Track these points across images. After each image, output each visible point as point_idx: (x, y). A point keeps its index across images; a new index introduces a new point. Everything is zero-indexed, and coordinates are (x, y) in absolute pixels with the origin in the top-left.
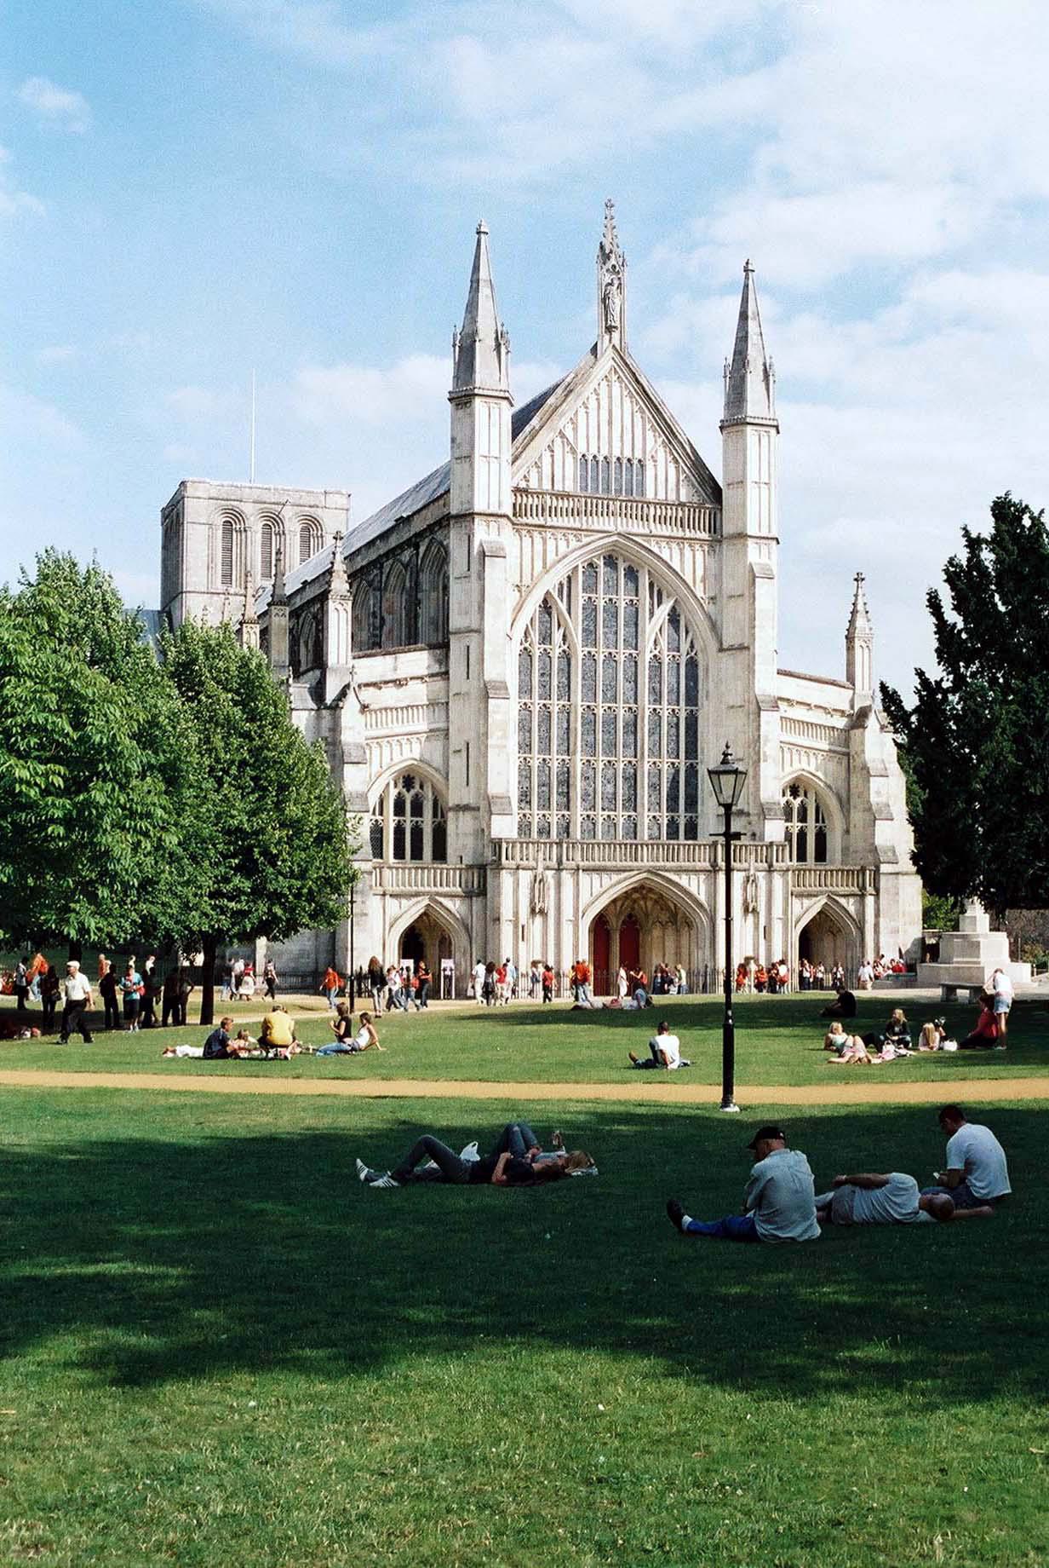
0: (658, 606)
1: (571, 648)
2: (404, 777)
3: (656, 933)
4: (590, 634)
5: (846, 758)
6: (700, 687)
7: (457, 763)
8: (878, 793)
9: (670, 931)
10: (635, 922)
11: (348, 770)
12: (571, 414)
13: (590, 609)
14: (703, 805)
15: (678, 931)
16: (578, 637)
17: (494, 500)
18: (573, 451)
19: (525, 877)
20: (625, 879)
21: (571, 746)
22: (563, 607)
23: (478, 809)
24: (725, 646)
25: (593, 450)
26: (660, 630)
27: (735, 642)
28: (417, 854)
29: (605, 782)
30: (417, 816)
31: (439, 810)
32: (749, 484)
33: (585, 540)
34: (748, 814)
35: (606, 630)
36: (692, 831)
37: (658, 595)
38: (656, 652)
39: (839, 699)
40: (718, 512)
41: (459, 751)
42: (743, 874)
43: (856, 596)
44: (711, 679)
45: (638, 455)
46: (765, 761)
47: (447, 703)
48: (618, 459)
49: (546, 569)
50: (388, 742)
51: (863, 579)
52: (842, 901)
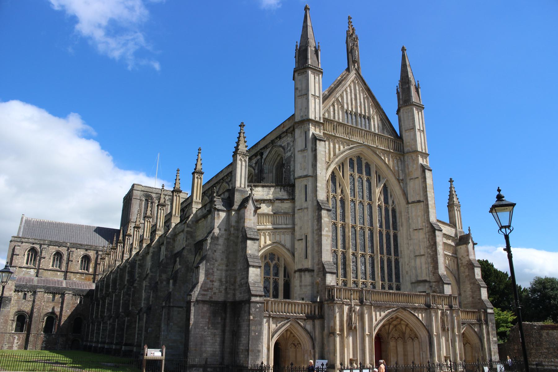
0: (379, 183)
1: (345, 196)
2: (270, 254)
3: (392, 344)
5: (456, 259)
6: (398, 221)
7: (299, 247)
9: (400, 342)
11: (249, 242)
12: (340, 93)
14: (403, 279)
15: (405, 342)
16: (348, 191)
17: (317, 116)
18: (343, 107)
19: (346, 308)
21: (347, 245)
23: (313, 271)
24: (410, 201)
27: (417, 199)
28: (276, 296)
29: (361, 264)
30: (275, 276)
31: (287, 274)
32: (417, 130)
33: (351, 146)
34: (429, 282)
35: (359, 190)
36: (398, 288)
37: (379, 179)
40: (401, 143)
41: (302, 239)
43: (451, 188)
44: (403, 217)
46: (439, 255)
47: (293, 215)
48: (360, 115)
50: (264, 233)
51: (453, 181)
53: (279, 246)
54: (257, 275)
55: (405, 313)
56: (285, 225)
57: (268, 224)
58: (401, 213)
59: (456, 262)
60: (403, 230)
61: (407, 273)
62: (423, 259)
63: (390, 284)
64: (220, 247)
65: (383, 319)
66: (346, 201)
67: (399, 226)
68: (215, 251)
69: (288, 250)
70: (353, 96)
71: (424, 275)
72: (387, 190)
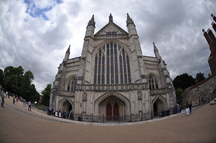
3: (121, 107)
4: (108, 54)
8: (165, 73)
13: (108, 50)
16: (105, 53)
18: (105, 32)
20: (106, 93)
22: (103, 51)
25: (109, 31)
33: (105, 40)
34: (140, 80)
37: (120, 47)
39: (156, 60)
42: (137, 91)
45: (116, 31)
46: (141, 67)
48: (112, 32)
49: (99, 44)
52: (162, 96)
54: (57, 83)
62: (137, 72)
65: (101, 96)
70: (110, 28)
71: (138, 78)
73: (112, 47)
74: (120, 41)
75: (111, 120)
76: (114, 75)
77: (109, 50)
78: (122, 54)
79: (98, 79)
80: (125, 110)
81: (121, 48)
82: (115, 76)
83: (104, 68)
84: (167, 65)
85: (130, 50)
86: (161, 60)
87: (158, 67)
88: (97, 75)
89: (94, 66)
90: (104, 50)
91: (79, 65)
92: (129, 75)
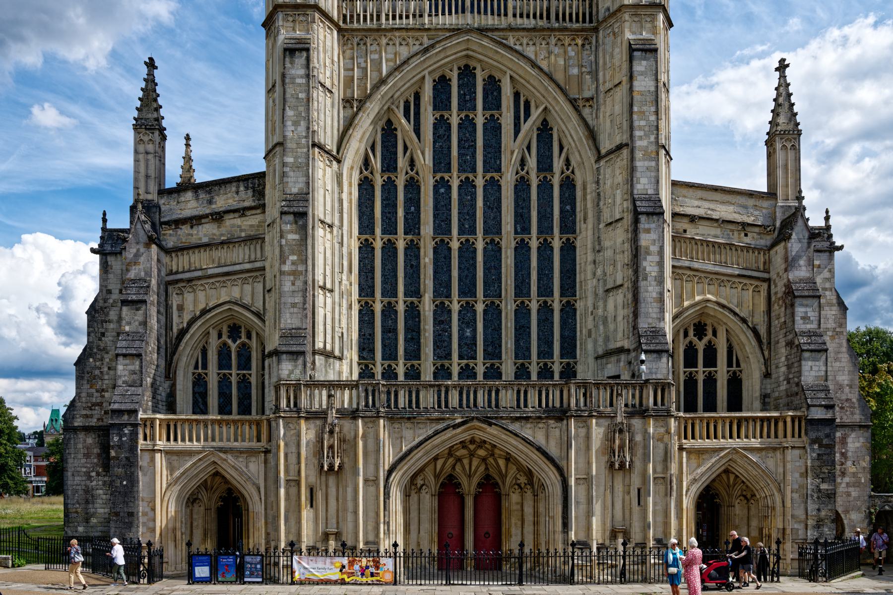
0: (525, 121)
6: (578, 209)
10: (496, 485)
13: (442, 126)
16: (426, 159)
26: (529, 148)
36: (569, 373)
37: (523, 108)
38: (523, 173)
44: (589, 197)
53: (236, 308)
55: (493, 430)
56: (249, 262)
57: (211, 266)
58: (585, 188)
59: (764, 293)
60: (587, 228)
61: (590, 331)
63: (546, 364)
64: (112, 326)
66: (422, 184)
67: (580, 221)
68: (103, 334)
69: (258, 315)
72: (552, 135)
73: (467, 103)
74: (530, 51)
75: (461, 567)
76: (480, 308)
77: (449, 127)
78: (532, 162)
79: (386, 330)
80: (536, 514)
81: (535, 114)
82: (485, 312)
83: (418, 257)
84: (841, 248)
85: (592, 135)
86: (800, 222)
87: (767, 263)
88: (378, 308)
89: (353, 245)
90: (417, 131)
91: (255, 239)
92: (569, 311)
